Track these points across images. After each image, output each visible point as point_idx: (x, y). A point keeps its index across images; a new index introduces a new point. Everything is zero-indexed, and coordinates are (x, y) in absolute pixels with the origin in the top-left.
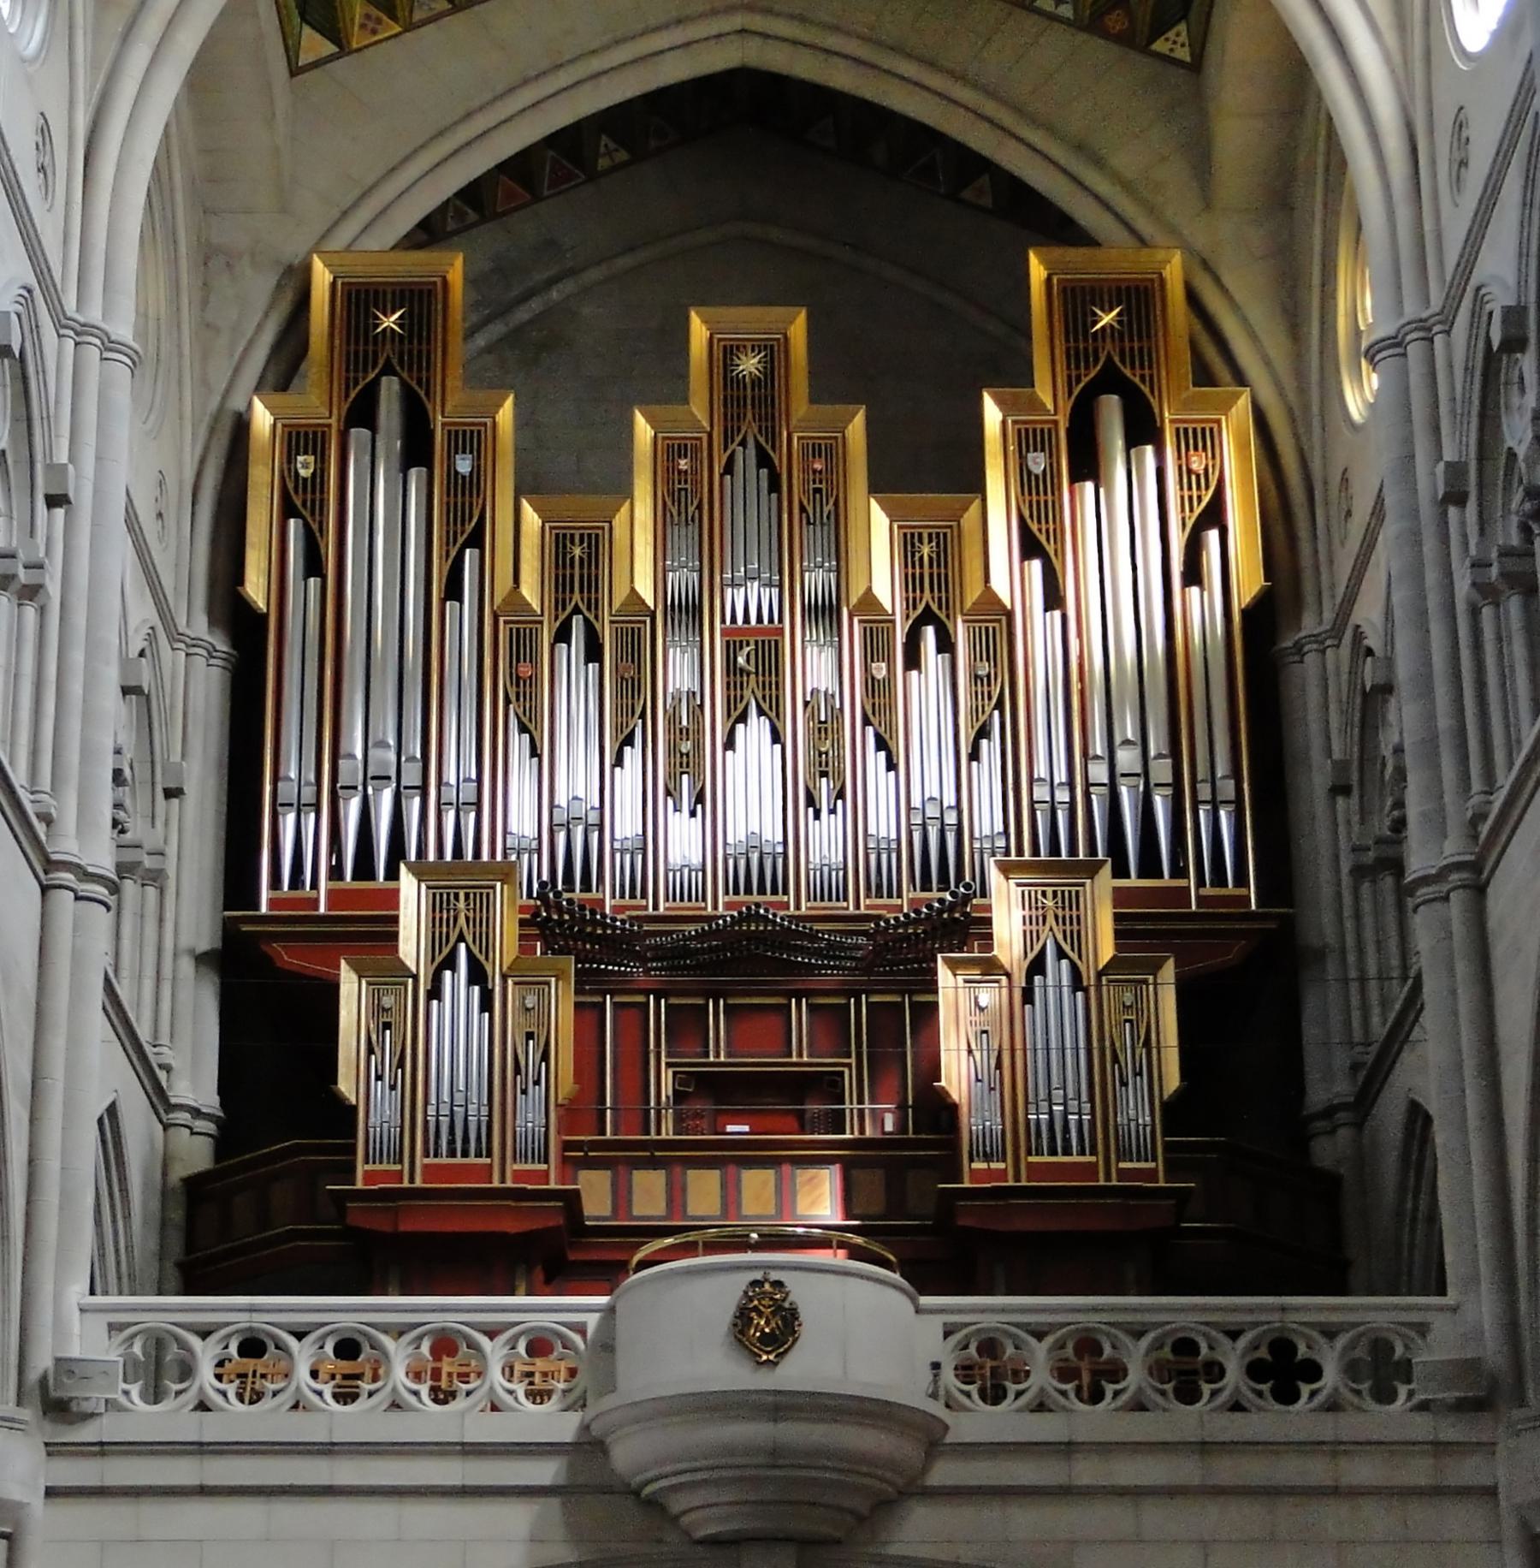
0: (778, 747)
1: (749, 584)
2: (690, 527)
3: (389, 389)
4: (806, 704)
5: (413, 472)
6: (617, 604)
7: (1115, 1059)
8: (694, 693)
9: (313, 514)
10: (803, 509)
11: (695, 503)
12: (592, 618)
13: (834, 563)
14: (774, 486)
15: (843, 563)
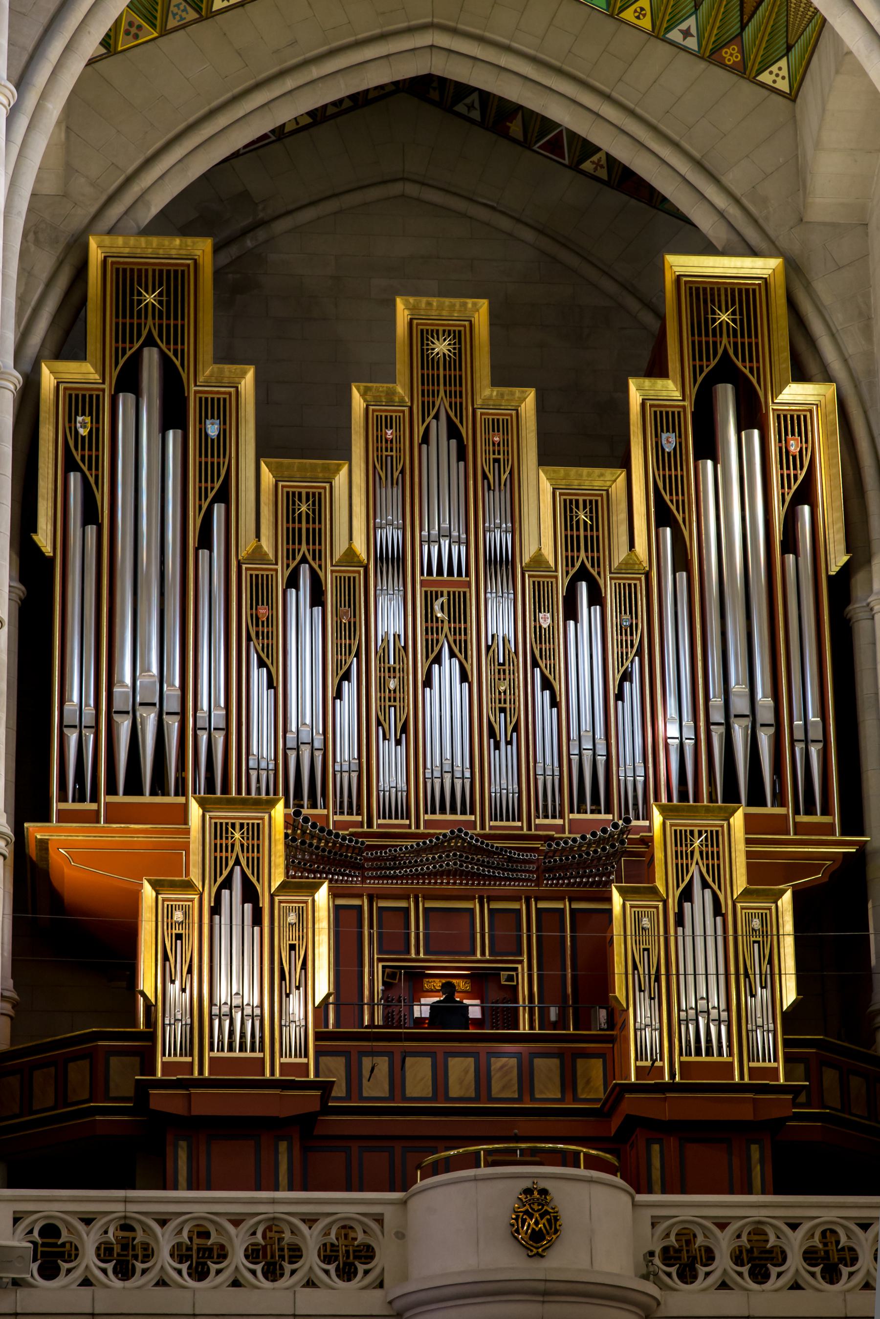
0: (466, 686)
1: (442, 542)
2: (395, 490)
3: (151, 360)
4: (488, 648)
5: (171, 434)
6: (337, 557)
7: (747, 975)
8: (399, 636)
9: (90, 469)
10: (485, 477)
11: (400, 468)
12: (316, 567)
13: (509, 525)
14: (462, 455)
15: (517, 525)
